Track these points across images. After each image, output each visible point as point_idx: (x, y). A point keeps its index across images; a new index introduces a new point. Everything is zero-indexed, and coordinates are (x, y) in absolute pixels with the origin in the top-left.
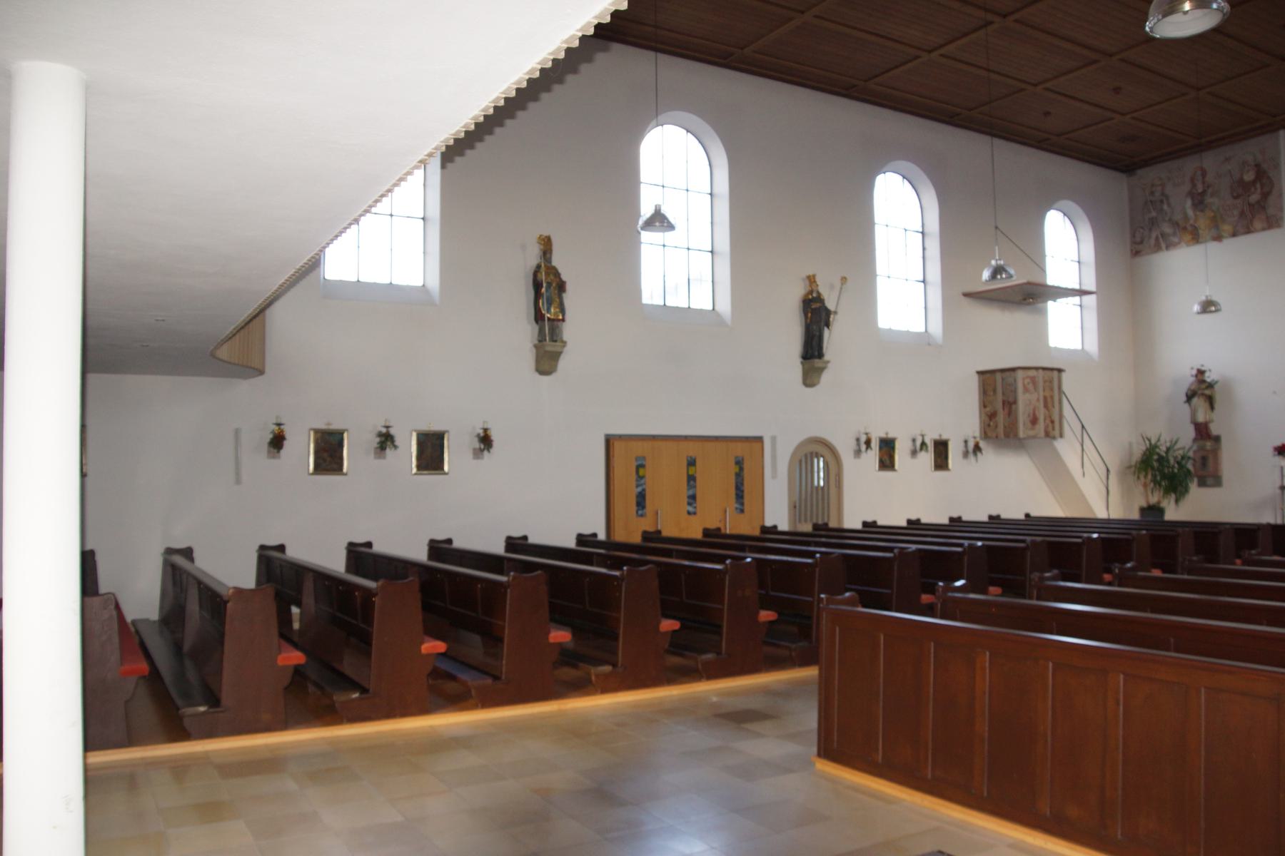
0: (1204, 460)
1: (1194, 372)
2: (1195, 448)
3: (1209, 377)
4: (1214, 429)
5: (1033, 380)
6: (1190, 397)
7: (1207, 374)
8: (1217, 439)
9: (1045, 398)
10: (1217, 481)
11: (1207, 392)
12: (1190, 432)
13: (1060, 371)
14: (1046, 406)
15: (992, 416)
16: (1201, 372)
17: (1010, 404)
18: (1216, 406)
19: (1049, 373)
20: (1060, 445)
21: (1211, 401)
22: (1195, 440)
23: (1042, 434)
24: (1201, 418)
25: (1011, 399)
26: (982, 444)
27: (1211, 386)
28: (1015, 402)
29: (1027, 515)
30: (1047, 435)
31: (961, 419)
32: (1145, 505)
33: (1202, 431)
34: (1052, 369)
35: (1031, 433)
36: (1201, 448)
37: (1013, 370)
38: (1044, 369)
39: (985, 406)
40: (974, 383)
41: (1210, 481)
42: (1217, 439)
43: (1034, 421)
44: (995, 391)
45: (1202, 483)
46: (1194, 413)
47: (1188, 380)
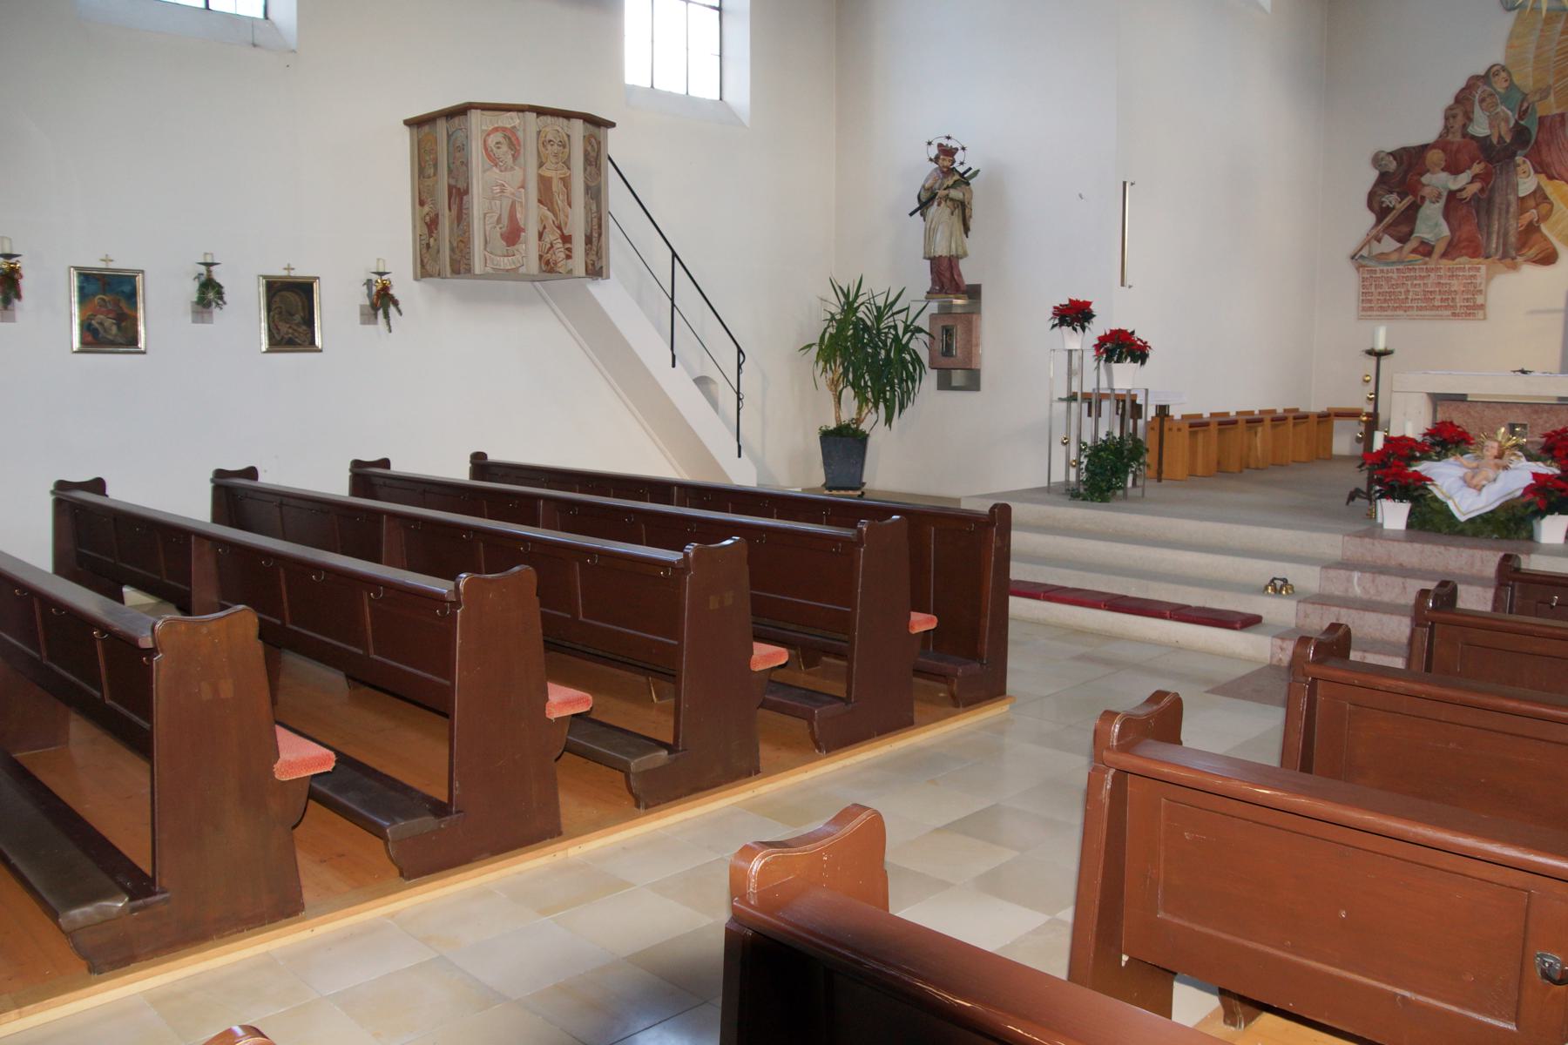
0: (948, 331)
1: (934, 151)
2: (933, 307)
3: (964, 162)
4: (969, 273)
5: (512, 140)
6: (924, 205)
7: (959, 157)
8: (974, 292)
9: (544, 183)
10: (973, 382)
11: (954, 193)
12: (925, 281)
13: (597, 123)
14: (545, 198)
15: (432, 224)
16: (947, 152)
17: (459, 194)
18: (972, 224)
19: (553, 125)
20: (608, 294)
21: (963, 210)
22: (931, 294)
23: (533, 266)
24: (941, 250)
25: (461, 185)
26: (404, 285)
27: (964, 180)
28: (466, 192)
29: (480, 465)
30: (548, 267)
31: (357, 222)
32: (833, 425)
33: (945, 275)
34: (568, 115)
35: (505, 263)
36: (946, 310)
37: (462, 111)
38: (541, 111)
39: (422, 203)
40: (402, 144)
41: (958, 377)
42: (974, 292)
43: (513, 235)
44: (435, 166)
45: (945, 384)
46: (929, 235)
47: (923, 170)
